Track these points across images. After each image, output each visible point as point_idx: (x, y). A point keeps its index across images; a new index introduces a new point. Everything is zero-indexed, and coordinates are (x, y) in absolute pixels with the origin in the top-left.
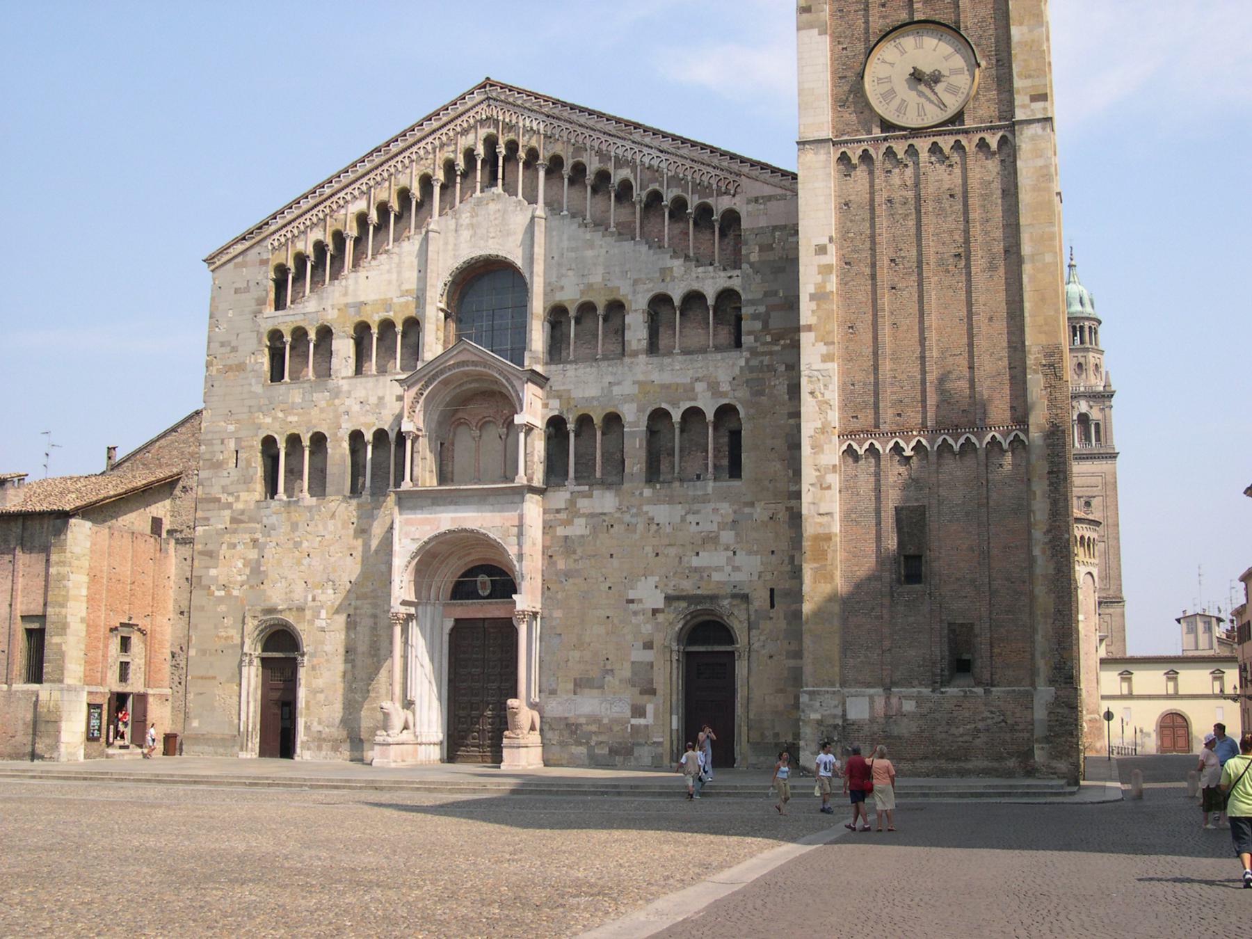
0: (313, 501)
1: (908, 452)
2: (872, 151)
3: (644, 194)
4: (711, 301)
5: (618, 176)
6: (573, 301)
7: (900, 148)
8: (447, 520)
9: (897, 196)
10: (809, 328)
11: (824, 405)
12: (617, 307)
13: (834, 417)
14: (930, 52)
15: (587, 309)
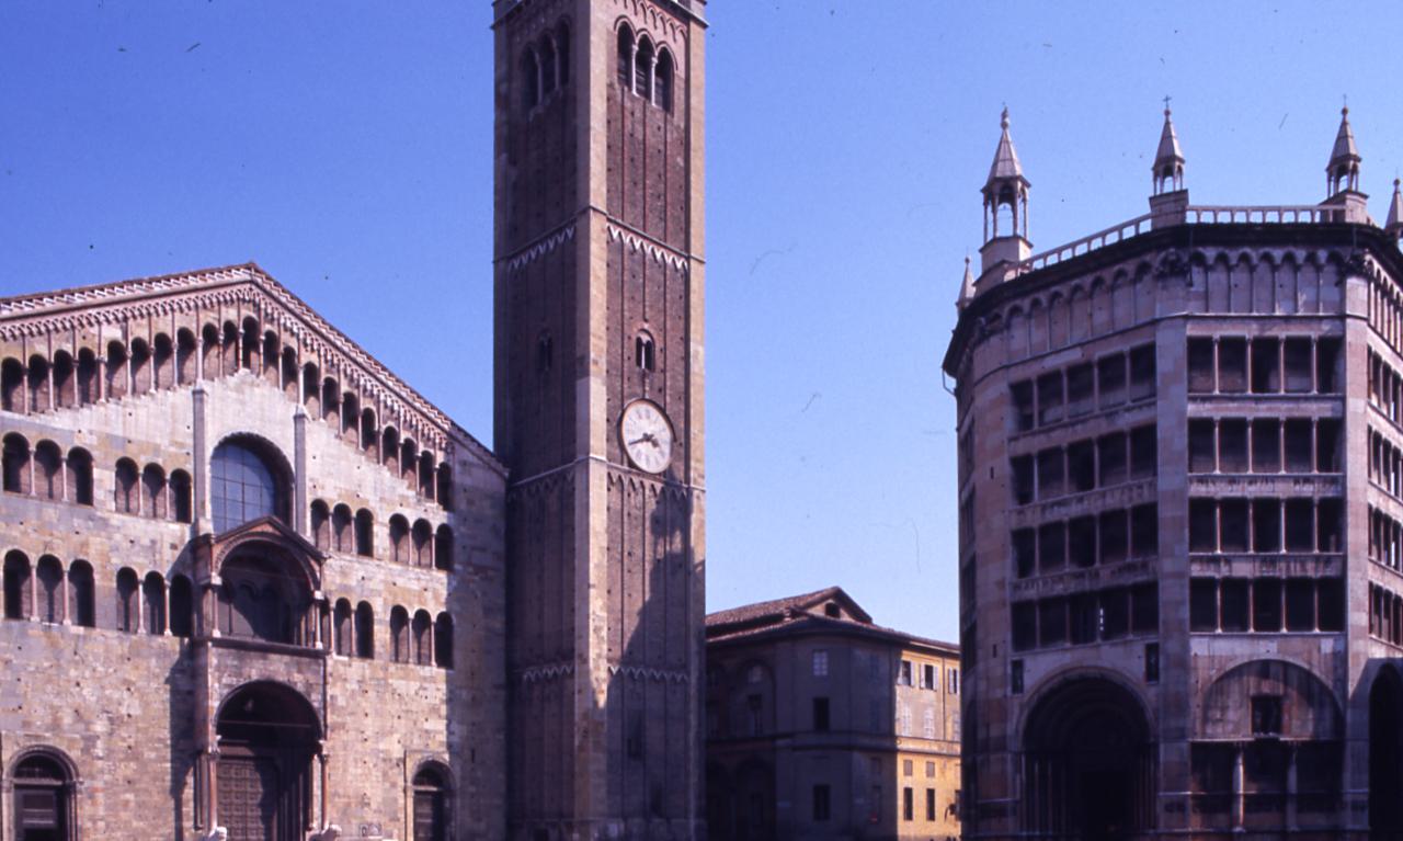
0: (81, 630)
1: (636, 677)
2: (623, 477)
3: (384, 427)
4: (435, 531)
5: (365, 404)
6: (332, 501)
7: (636, 480)
8: (255, 670)
9: (635, 512)
10: (594, 586)
11: (600, 639)
12: (365, 519)
13: (605, 647)
14: (655, 424)
15: (342, 510)
